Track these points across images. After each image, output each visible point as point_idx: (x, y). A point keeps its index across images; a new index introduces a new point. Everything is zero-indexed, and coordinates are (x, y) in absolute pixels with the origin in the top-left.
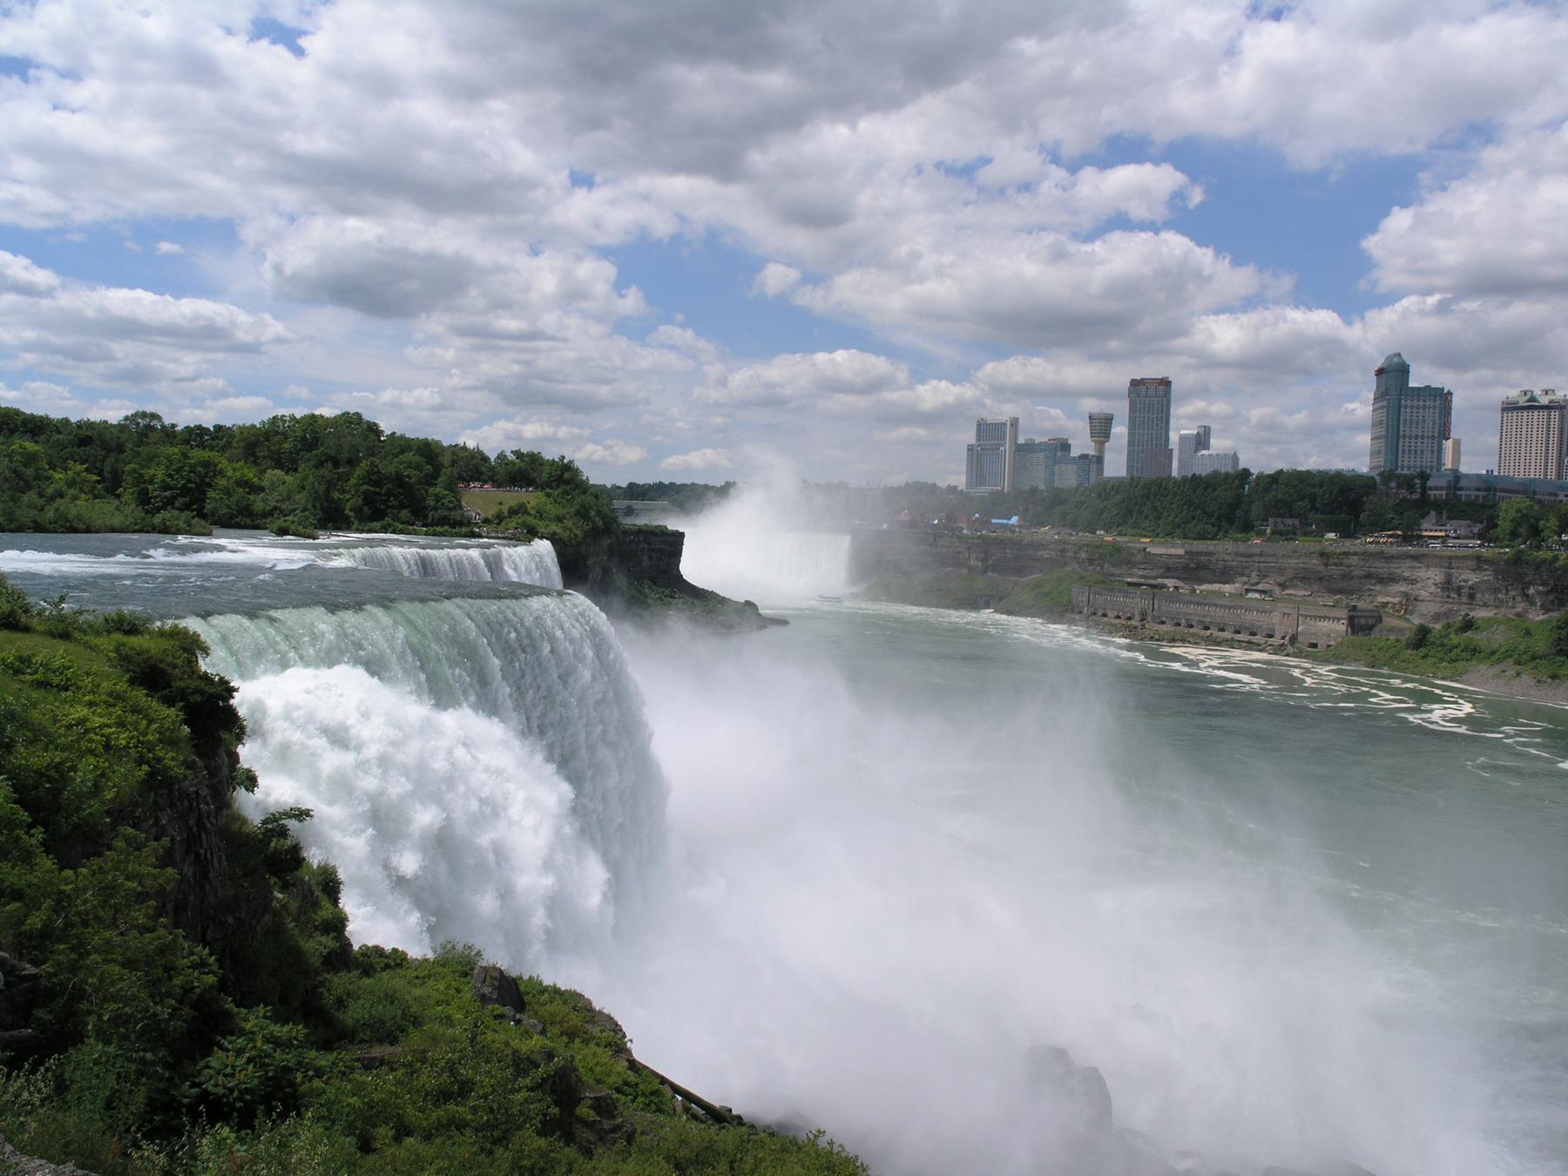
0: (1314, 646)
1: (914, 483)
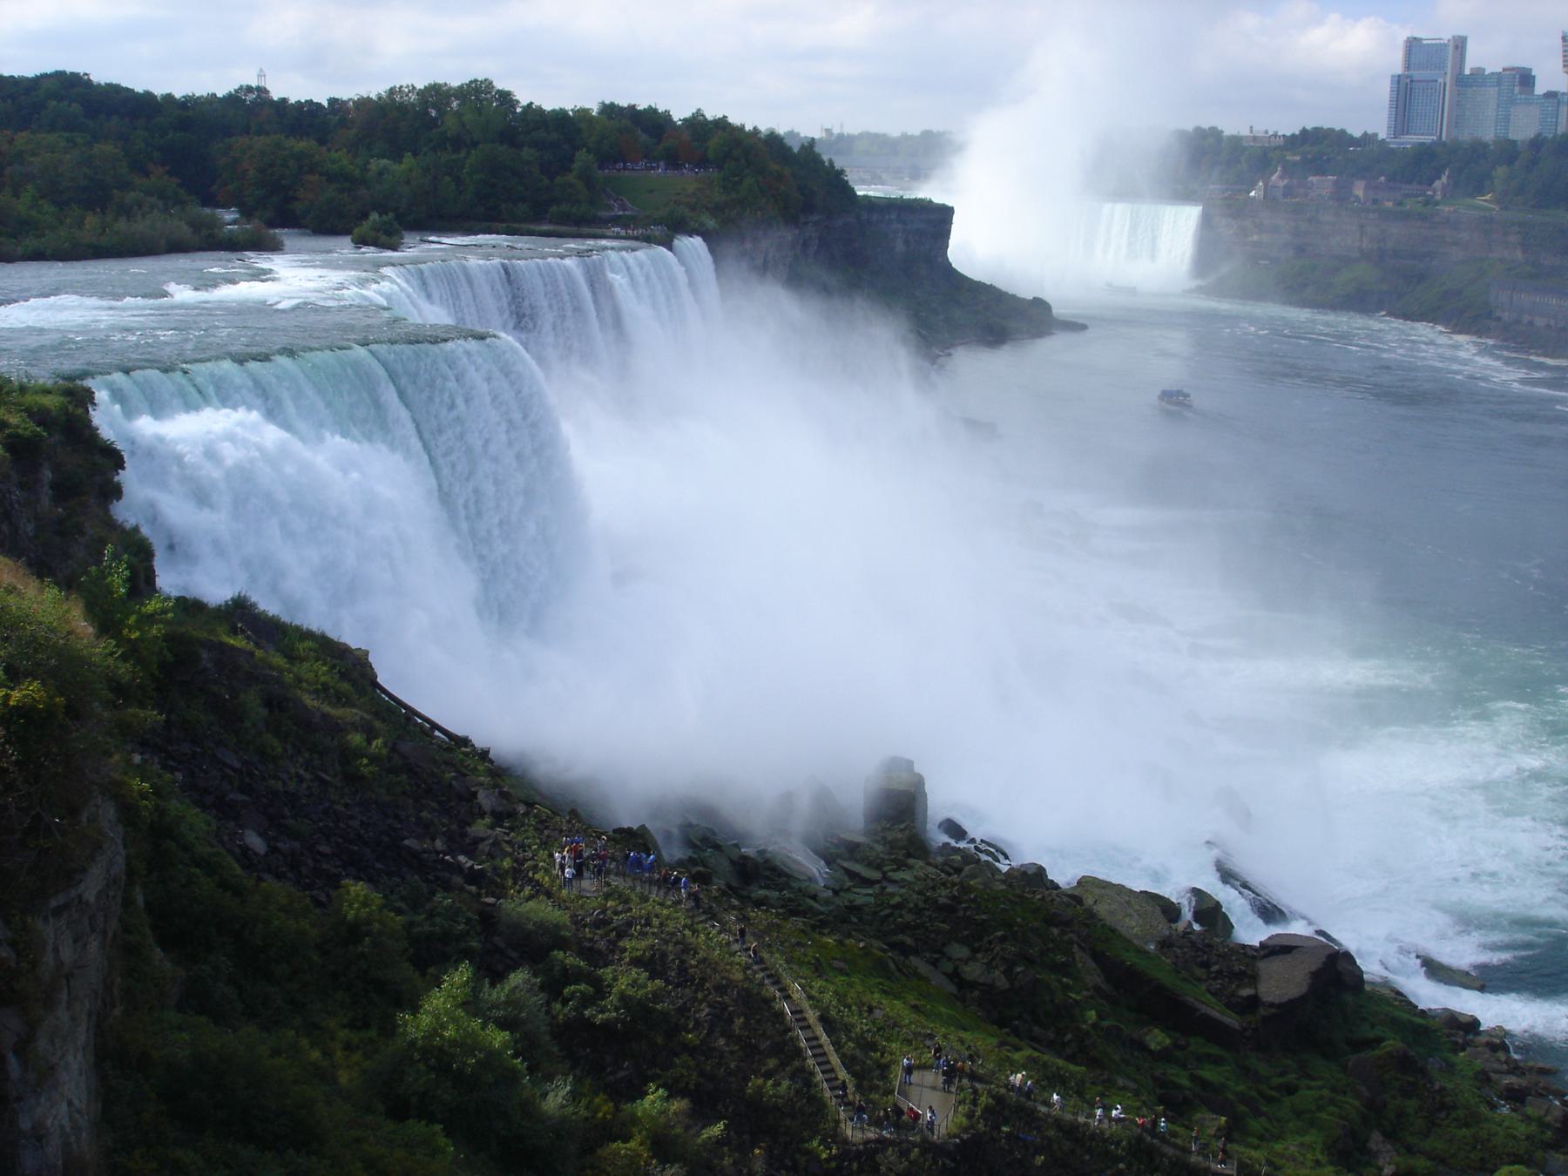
1: (1316, 130)
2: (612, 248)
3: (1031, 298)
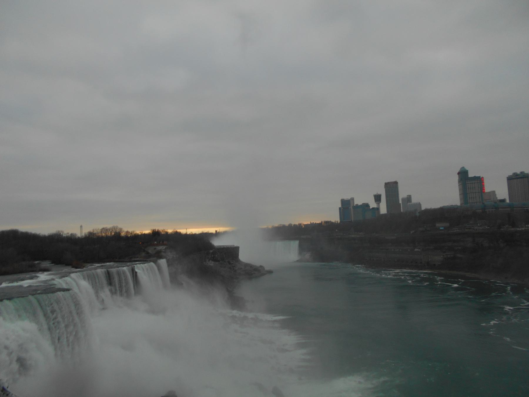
0: (435, 265)
2: (138, 264)
3: (259, 265)
